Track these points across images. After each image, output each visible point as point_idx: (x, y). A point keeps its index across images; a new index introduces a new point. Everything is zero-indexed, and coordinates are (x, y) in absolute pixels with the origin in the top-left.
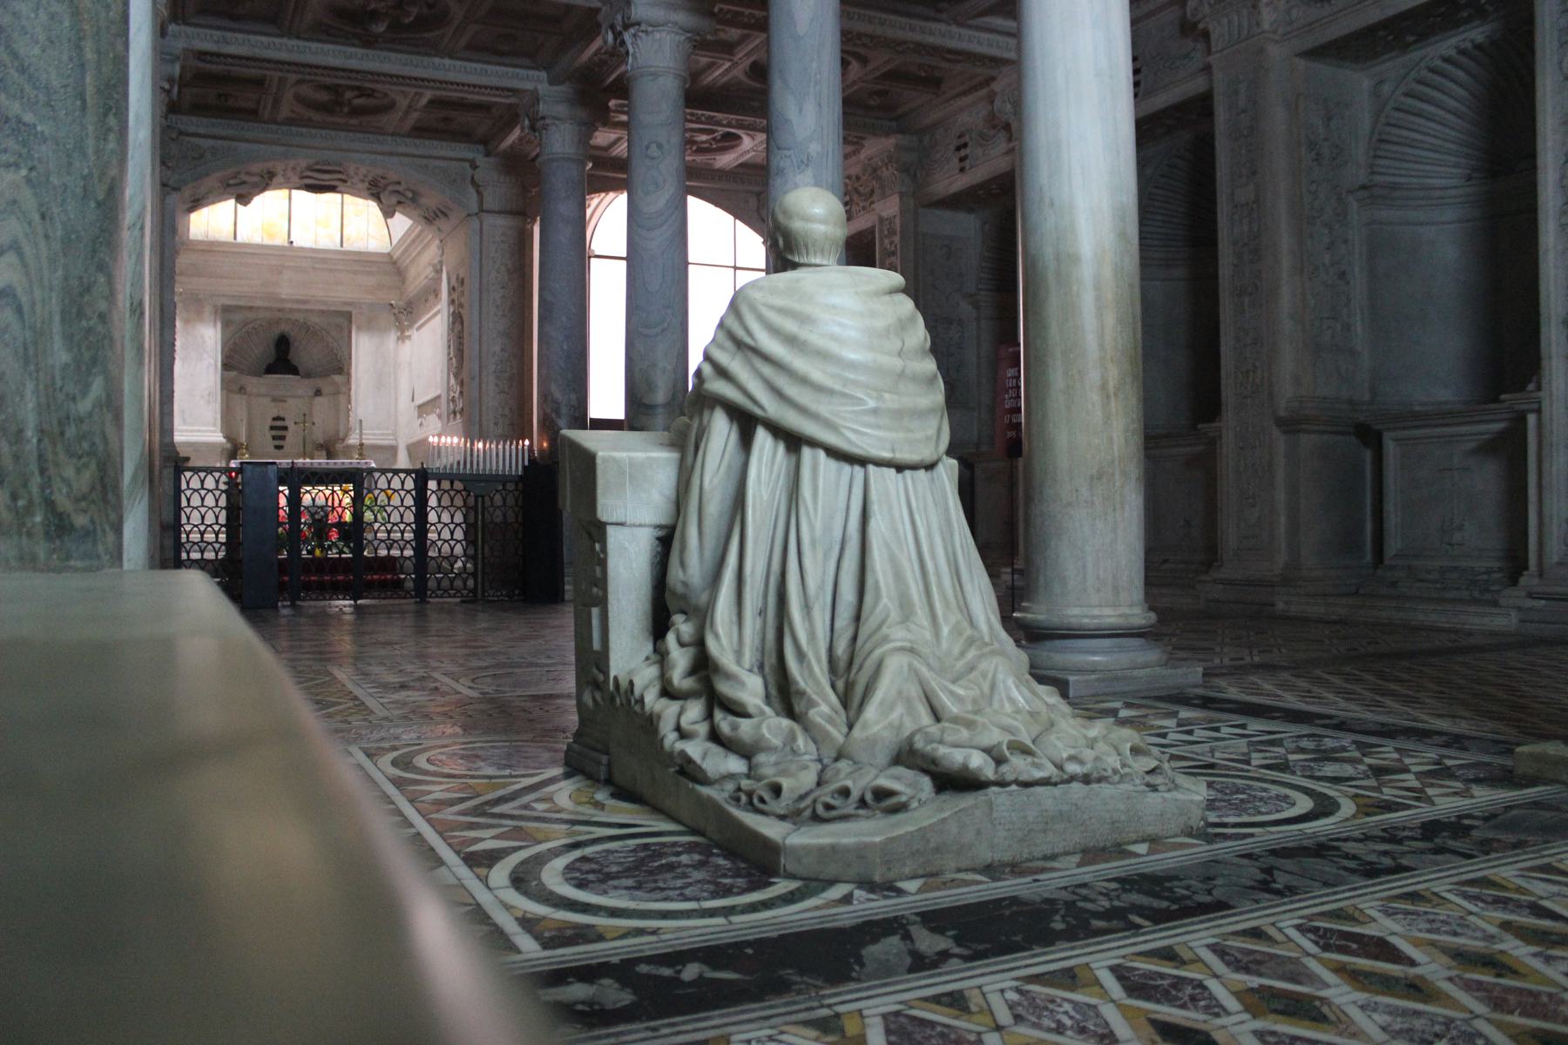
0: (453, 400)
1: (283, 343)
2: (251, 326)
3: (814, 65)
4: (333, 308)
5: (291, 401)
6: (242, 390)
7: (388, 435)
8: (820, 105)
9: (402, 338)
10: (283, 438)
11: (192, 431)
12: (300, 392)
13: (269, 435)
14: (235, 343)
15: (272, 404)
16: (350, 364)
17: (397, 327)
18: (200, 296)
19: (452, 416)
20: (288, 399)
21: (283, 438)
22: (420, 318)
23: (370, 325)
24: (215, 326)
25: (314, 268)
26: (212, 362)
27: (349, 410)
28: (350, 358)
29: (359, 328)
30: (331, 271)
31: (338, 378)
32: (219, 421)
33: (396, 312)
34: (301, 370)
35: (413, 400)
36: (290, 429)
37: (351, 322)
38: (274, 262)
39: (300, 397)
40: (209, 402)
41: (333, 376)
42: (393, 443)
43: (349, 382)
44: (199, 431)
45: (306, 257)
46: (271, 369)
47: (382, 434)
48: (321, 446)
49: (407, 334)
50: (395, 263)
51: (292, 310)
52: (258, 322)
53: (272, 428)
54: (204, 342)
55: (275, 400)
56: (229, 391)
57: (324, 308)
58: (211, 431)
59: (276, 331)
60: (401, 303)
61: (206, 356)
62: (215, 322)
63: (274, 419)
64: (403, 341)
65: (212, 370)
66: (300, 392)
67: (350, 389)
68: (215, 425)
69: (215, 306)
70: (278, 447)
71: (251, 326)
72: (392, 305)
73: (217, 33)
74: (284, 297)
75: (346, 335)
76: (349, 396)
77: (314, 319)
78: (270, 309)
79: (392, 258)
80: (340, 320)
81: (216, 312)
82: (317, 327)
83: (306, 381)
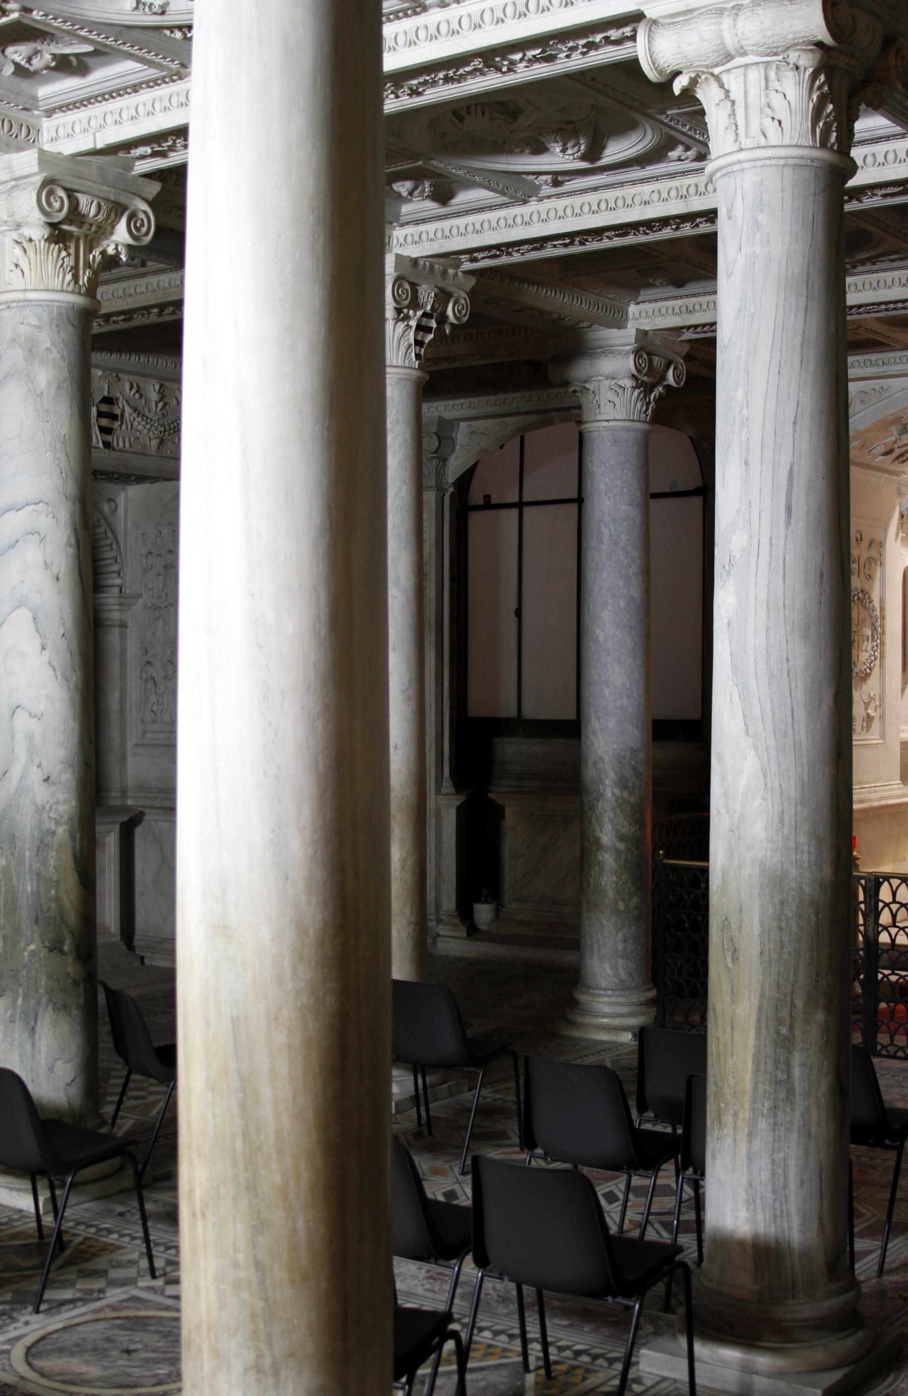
3: (740, 394)
8: (746, 463)
73: (680, 302)
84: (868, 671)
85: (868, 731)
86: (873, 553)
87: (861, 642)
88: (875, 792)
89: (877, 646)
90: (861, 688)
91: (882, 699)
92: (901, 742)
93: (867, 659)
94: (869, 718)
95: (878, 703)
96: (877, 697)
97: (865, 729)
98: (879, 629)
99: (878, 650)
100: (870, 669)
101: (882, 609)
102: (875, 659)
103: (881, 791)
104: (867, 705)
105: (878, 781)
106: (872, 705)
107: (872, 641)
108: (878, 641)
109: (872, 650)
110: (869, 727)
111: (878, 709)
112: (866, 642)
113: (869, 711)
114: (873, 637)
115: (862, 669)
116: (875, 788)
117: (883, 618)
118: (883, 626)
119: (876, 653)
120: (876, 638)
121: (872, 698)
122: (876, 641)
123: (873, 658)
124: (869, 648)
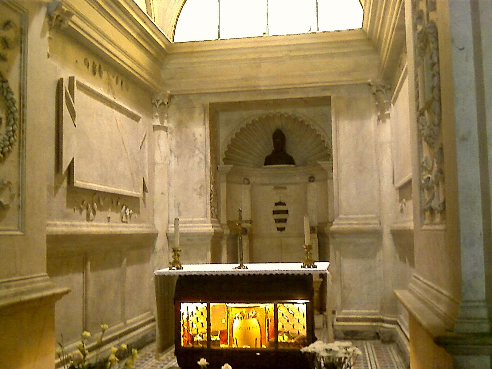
4: (311, 95)
5: (291, 189)
7: (373, 218)
9: (382, 118)
10: (285, 221)
13: (272, 218)
18: (191, 97)
19: (428, 214)
20: (288, 187)
21: (285, 221)
24: (205, 124)
25: (291, 58)
30: (305, 57)
31: (323, 164)
33: (374, 89)
34: (297, 162)
36: (290, 213)
39: (296, 184)
40: (200, 195)
42: (377, 227)
44: (191, 222)
46: (269, 161)
49: (387, 112)
51: (277, 103)
53: (274, 212)
54: (196, 139)
55: (276, 188)
56: (228, 182)
58: (202, 222)
61: (197, 152)
63: (276, 204)
64: (384, 121)
65: (202, 164)
66: (298, 179)
69: (203, 105)
70: (281, 229)
72: (369, 84)
74: (263, 88)
77: (302, 112)
81: (205, 111)
86: (10, 34)
88: (8, 287)
91: (21, 187)
101: (22, 96)
102: (11, 144)
103: (16, 286)
105: (14, 275)
107: (8, 124)
109: (7, 134)
116: (8, 284)
117: (23, 106)
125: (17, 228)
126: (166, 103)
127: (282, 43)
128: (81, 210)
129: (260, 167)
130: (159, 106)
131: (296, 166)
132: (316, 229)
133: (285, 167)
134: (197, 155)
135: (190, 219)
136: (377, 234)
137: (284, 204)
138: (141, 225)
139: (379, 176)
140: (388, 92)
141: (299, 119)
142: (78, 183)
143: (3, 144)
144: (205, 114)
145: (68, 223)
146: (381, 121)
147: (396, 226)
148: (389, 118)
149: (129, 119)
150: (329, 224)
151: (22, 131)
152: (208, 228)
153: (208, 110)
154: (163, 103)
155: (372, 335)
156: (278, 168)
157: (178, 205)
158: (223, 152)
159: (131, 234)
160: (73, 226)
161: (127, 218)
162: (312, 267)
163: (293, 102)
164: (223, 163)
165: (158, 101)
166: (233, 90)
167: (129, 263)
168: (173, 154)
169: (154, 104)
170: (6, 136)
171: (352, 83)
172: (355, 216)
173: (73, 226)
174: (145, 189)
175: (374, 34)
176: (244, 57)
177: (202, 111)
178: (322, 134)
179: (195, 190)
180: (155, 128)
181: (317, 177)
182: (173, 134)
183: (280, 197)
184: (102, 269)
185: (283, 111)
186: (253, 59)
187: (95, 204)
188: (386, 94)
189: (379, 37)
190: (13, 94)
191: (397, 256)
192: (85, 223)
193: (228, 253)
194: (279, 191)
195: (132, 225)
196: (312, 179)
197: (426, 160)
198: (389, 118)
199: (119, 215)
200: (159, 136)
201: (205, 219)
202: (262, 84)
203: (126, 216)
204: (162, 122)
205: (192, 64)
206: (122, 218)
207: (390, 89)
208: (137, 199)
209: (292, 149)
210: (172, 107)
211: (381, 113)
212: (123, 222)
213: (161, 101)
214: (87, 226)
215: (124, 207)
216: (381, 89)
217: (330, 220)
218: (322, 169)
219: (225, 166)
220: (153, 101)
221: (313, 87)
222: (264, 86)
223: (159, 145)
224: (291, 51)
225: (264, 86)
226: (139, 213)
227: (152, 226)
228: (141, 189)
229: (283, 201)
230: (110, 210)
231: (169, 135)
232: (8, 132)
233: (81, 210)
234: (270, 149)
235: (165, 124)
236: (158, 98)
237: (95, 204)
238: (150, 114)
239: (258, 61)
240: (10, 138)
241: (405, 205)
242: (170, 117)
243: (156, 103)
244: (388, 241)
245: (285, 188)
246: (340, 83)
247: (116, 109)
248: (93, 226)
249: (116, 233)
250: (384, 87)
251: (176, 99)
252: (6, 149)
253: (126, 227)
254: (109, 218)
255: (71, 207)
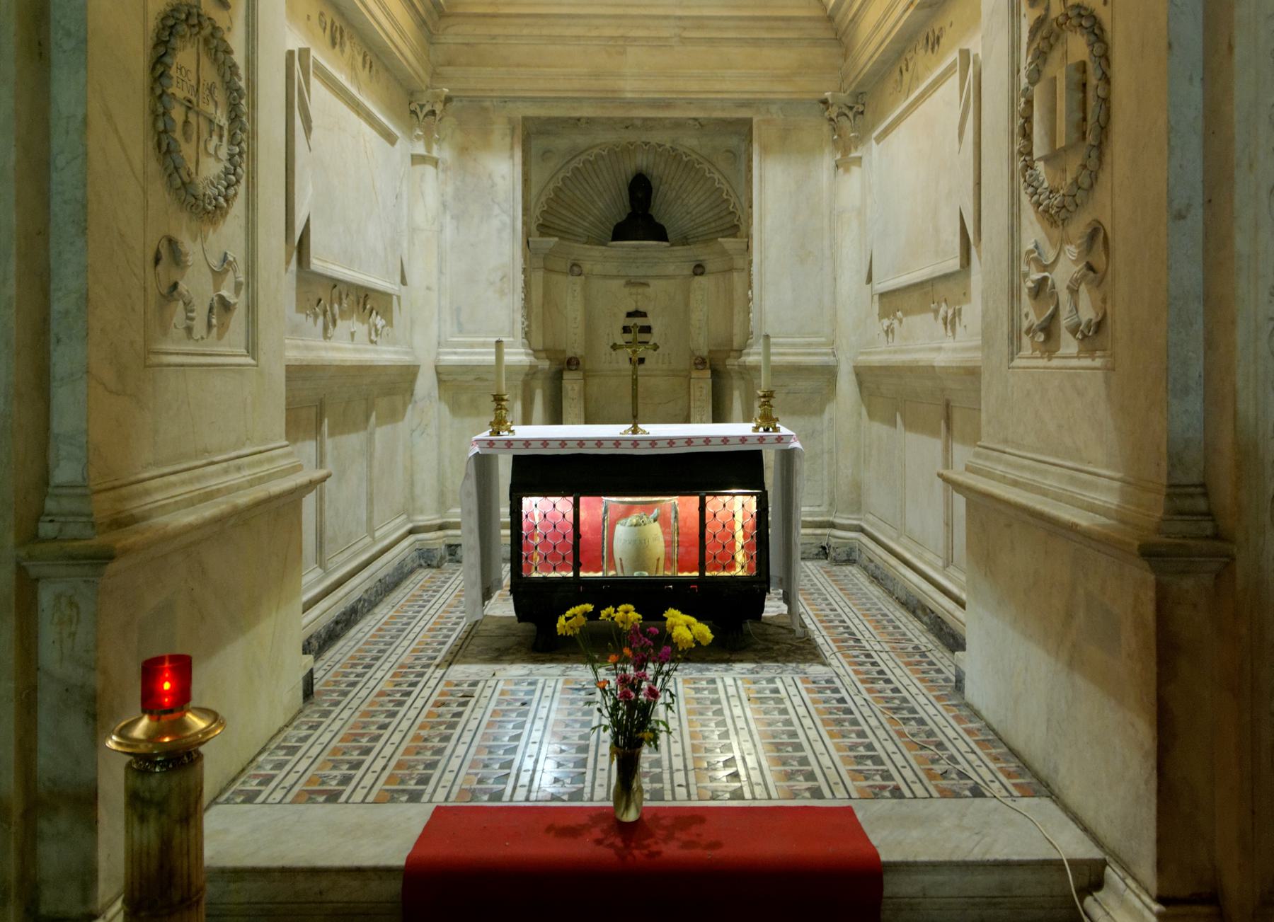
0: (1040, 289)
1: (641, 188)
2: (583, 157)
4: (718, 114)
5: (656, 286)
6: (575, 268)
9: (843, 165)
11: (472, 345)
12: (671, 269)
14: (558, 190)
15: (627, 290)
16: (750, 216)
17: (834, 142)
18: (487, 104)
20: (652, 282)
22: (882, 116)
23: (786, 142)
24: (512, 157)
25: (683, 41)
26: (507, 220)
27: (750, 300)
28: (751, 207)
29: (765, 150)
30: (711, 41)
31: (729, 243)
32: (519, 327)
33: (833, 112)
34: (669, 236)
35: (869, 279)
36: (655, 330)
37: (751, 141)
38: (608, 32)
40: (502, 293)
41: (719, 239)
42: (829, 360)
43: (748, 248)
45: (666, 17)
46: (621, 232)
47: (809, 345)
48: (703, 362)
49: (854, 154)
50: (830, 19)
51: (648, 124)
52: (596, 151)
53: (626, 330)
55: (629, 284)
56: (547, 270)
57: (700, 114)
59: (630, 167)
60: (844, 97)
61: (496, 210)
62: (512, 148)
63: (629, 315)
64: (847, 170)
65: (506, 235)
66: (671, 269)
67: (751, 262)
68: (513, 337)
69: (510, 121)
71: (583, 157)
72: (825, 102)
74: (629, 95)
75: (743, 167)
76: (750, 275)
77: (689, 141)
78: (610, 123)
79: (825, 7)
80: (733, 142)
81: (513, 130)
82: (694, 156)
83: (680, 251)
84: (221, 200)
85: (220, 337)
87: (205, 135)
89: (240, 154)
90: (205, 239)
91: (251, 270)
92: (287, 366)
93: (219, 177)
94: (226, 306)
95: (242, 279)
96: (241, 267)
97: (215, 330)
98: (244, 119)
99: (244, 166)
100: (227, 200)
102: (238, 181)
104: (218, 275)
106: (229, 280)
108: (244, 145)
110: (223, 327)
111: (243, 292)
112: (215, 138)
113: (224, 293)
114: (233, 136)
115: (208, 192)
118: (254, 121)
119: (239, 170)
120: (239, 137)
121: (230, 263)
122: (238, 145)
123: (233, 178)
124: (223, 153)
125: (246, 354)
126: (437, 112)
127: (669, 12)
128: (316, 317)
129: (604, 244)
130: (426, 115)
131: (672, 245)
132: (708, 361)
133: (652, 246)
134: (496, 216)
135: (482, 339)
136: (829, 373)
137: (644, 315)
138: (396, 349)
139: (834, 270)
140: (859, 116)
141: (684, 157)
142: (316, 264)
143: (225, 181)
144: (512, 138)
145: (300, 342)
146: (841, 170)
147: (860, 358)
148: (860, 166)
149: (382, 140)
150: (732, 354)
151: (253, 158)
152: (517, 356)
153: (519, 132)
154: (433, 113)
155: (815, 551)
156: (637, 248)
157: (457, 311)
158: (538, 212)
159: (385, 366)
160: (307, 348)
161: (377, 335)
162: (771, 430)
163: (678, 124)
164: (538, 233)
165: (422, 107)
166: (570, 94)
167: (380, 423)
168: (448, 212)
169: (413, 112)
170: (228, 165)
171: (795, 96)
172: (790, 340)
173: (307, 348)
174: (404, 281)
175: (843, 10)
176: (595, 33)
177: (508, 132)
178: (725, 187)
179: (492, 284)
180: (417, 159)
181: (709, 267)
182: (449, 173)
183: (636, 302)
184: (342, 433)
185: (656, 137)
186: (611, 38)
187: (336, 306)
188: (854, 120)
189: (855, 15)
190: (240, 79)
191: (864, 412)
192: (321, 343)
193: (544, 404)
194: (634, 290)
195: (384, 348)
196: (699, 271)
197: (1037, 247)
198: (860, 166)
199: (366, 326)
200: (423, 175)
201: (511, 339)
202: (628, 88)
203: (376, 330)
204: (429, 149)
205: (494, 37)
206: (370, 334)
207: (862, 113)
208: (390, 295)
209: (661, 211)
210: (449, 121)
211: (842, 156)
212: (372, 342)
213: (428, 108)
214: (326, 349)
215: (374, 313)
216: (847, 111)
217: (736, 345)
218: (724, 253)
219: (541, 239)
220: (413, 107)
221: (722, 100)
222: (632, 91)
223: (422, 194)
224: (685, 29)
225: (632, 91)
226: (392, 326)
227: (410, 350)
228: (398, 279)
229: (641, 309)
230: (355, 316)
231: (441, 175)
232: (231, 156)
233: (316, 317)
234: (620, 209)
235: (435, 154)
236: (424, 102)
237: (336, 306)
238: (408, 130)
239: (621, 43)
240: (235, 170)
241: (901, 322)
242: (444, 139)
243: (418, 110)
244: (846, 385)
245: (646, 285)
246: (772, 96)
247: (366, 120)
248: (334, 349)
249: (522, 364)
250: (851, 108)
251: (455, 103)
252: (231, 191)
253: (376, 351)
254: (353, 334)
255: (301, 312)
